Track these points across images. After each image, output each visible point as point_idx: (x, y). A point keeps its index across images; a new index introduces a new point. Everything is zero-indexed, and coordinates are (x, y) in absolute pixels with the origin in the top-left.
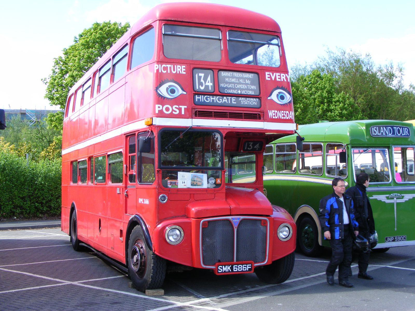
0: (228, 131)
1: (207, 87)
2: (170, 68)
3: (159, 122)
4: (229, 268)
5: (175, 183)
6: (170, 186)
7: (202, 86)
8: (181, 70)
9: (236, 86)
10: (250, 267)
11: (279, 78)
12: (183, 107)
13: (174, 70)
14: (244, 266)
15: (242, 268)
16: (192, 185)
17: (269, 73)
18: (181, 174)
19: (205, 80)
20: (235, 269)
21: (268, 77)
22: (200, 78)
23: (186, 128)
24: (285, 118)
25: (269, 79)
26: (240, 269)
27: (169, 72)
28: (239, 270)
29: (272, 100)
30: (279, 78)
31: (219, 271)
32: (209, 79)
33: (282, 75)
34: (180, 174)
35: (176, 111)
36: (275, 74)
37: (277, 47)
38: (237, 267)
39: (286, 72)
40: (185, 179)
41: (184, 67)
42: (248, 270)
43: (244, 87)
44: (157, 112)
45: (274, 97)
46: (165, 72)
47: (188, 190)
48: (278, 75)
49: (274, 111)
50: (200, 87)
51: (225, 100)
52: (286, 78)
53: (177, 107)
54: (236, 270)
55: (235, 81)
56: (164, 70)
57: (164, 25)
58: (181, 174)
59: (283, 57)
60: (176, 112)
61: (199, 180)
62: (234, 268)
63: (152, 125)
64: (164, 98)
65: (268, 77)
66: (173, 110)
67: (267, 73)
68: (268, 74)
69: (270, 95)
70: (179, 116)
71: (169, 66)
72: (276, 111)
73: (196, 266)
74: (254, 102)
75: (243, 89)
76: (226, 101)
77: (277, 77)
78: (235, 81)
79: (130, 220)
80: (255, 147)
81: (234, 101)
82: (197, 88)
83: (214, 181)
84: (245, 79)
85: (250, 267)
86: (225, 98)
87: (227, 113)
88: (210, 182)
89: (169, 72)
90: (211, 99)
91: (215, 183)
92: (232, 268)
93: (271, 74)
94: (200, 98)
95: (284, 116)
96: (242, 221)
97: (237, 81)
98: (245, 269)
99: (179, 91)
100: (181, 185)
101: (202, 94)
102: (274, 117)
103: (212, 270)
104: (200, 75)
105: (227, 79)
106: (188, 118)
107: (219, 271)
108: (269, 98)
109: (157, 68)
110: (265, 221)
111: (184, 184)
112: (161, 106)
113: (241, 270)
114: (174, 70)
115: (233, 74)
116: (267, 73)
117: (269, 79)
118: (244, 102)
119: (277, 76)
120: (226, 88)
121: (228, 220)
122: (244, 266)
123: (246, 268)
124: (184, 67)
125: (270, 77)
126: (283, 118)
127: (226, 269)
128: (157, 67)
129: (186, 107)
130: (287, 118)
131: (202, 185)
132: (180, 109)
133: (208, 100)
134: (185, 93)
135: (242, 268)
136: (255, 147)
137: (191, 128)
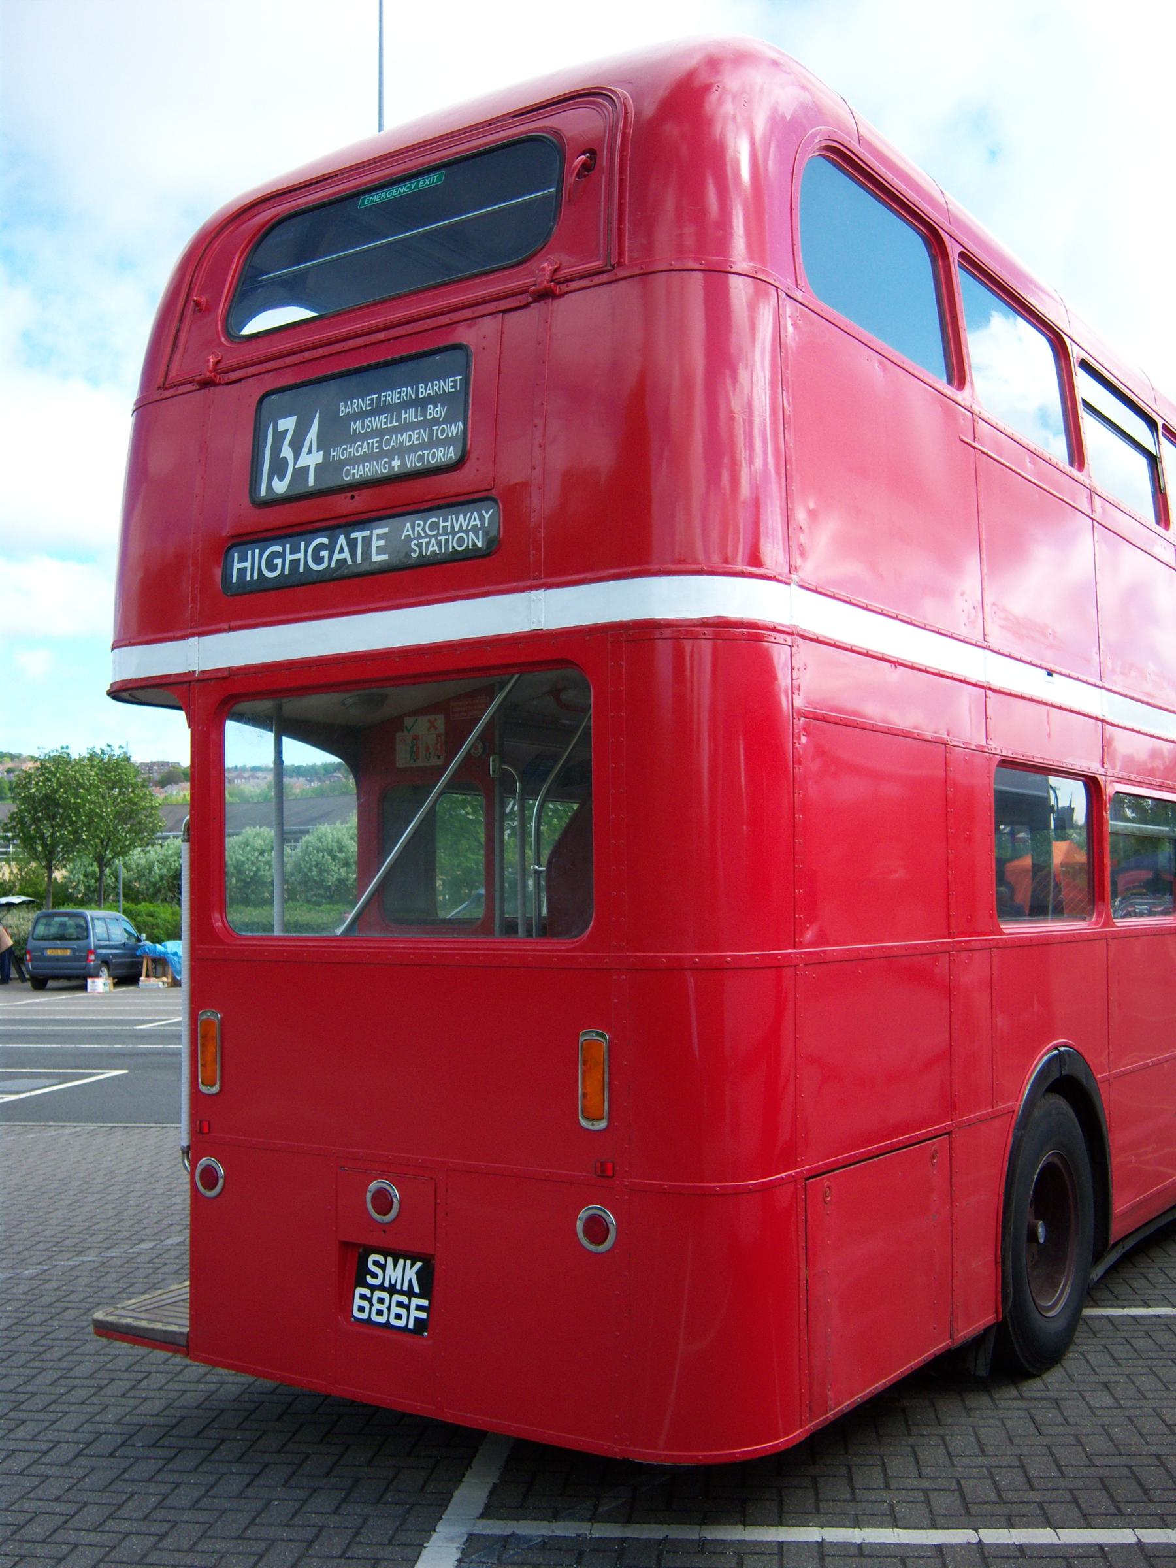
10: (423, 1315)
14: (400, 1304)
15: (389, 1308)
20: (361, 1309)
38: (370, 1300)
42: (411, 1326)
43: (418, 439)
55: (386, 423)
78: (386, 423)
85: (423, 1315)
97: (392, 422)
98: (398, 1316)
115: (378, 399)
122: (400, 1304)
123: (403, 1311)
135: (389, 1308)
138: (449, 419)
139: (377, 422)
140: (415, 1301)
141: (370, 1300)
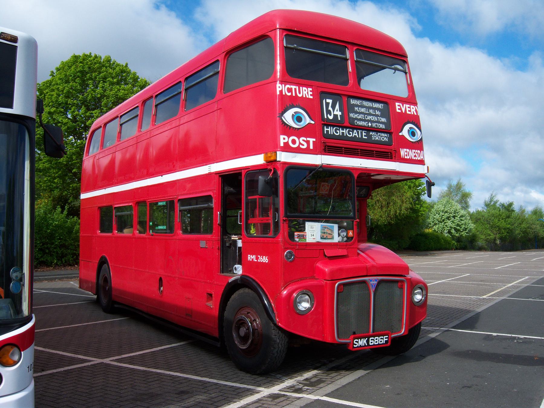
1: (336, 116)
2: (295, 89)
3: (283, 157)
4: (365, 341)
5: (303, 235)
6: (297, 240)
7: (330, 115)
8: (308, 93)
9: (367, 117)
11: (409, 111)
12: (312, 140)
13: (300, 93)
16: (321, 238)
17: (399, 104)
18: (308, 225)
19: (333, 107)
20: (372, 343)
21: (399, 109)
22: (327, 104)
23: (316, 166)
25: (400, 111)
26: (376, 342)
27: (294, 95)
28: (375, 343)
29: (403, 136)
30: (409, 111)
31: (355, 346)
32: (337, 107)
33: (412, 107)
34: (308, 225)
35: (303, 145)
36: (405, 105)
37: (403, 74)
38: (374, 340)
39: (415, 104)
40: (314, 231)
41: (311, 89)
44: (282, 145)
45: (405, 133)
46: (289, 94)
47: (318, 244)
48: (409, 107)
49: (405, 150)
50: (329, 115)
51: (355, 134)
52: (416, 111)
53: (305, 139)
54: (372, 344)
56: (289, 92)
57: (286, 35)
58: (308, 225)
59: (411, 87)
60: (303, 145)
61: (329, 232)
62: (370, 341)
63: (275, 161)
64: (290, 127)
65: (399, 109)
66: (300, 143)
67: (397, 104)
68: (398, 106)
69: (401, 131)
70: (307, 151)
71: (293, 87)
72: (408, 150)
73: (329, 340)
74: (384, 137)
76: (356, 135)
77: (408, 109)
79: (230, 281)
80: (361, 193)
81: (365, 136)
82: (326, 117)
83: (345, 234)
84: (375, 109)
86: (355, 131)
87: (358, 149)
88: (342, 234)
89: (294, 95)
90: (341, 131)
91: (347, 236)
92: (368, 341)
93: (401, 104)
94: (329, 129)
95: (415, 156)
96: (380, 282)
98: (381, 341)
99: (307, 120)
100: (309, 239)
101: (331, 125)
102: (406, 157)
103: (345, 344)
104: (328, 101)
105: (356, 109)
106: (317, 154)
107: (355, 346)
109: (281, 89)
110: (402, 281)
111: (313, 237)
112: (286, 137)
113: (377, 343)
114: (300, 93)
116: (397, 104)
117: (400, 111)
118: (376, 137)
119: (406, 108)
120: (356, 119)
121: (364, 282)
124: (311, 89)
125: (400, 109)
126: (414, 158)
127: (362, 342)
128: (279, 87)
129: (314, 140)
130: (419, 159)
131: (332, 238)
132: (308, 142)
133: (337, 133)
134: (313, 122)
136: (361, 193)
137: (322, 166)
138: (382, 116)
139: (363, 110)
140: (385, 337)
141: (374, 340)
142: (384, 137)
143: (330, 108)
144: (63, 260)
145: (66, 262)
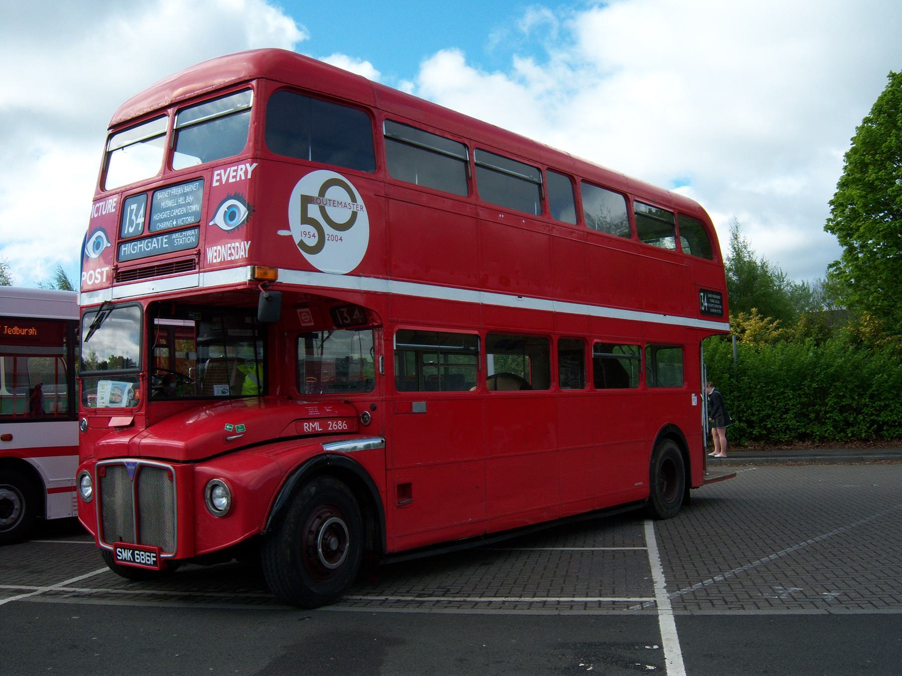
0: (151, 300)
4: (130, 555)
22: (132, 211)
24: (233, 258)
32: (142, 212)
33: (240, 167)
75: (181, 216)
86: (155, 239)
95: (231, 255)
102: (215, 261)
108: (211, 224)
121: (122, 465)
125: (220, 180)
126: (229, 259)
130: (237, 257)
142: (190, 237)
143: (134, 217)
144: (849, 431)
145: (853, 435)
